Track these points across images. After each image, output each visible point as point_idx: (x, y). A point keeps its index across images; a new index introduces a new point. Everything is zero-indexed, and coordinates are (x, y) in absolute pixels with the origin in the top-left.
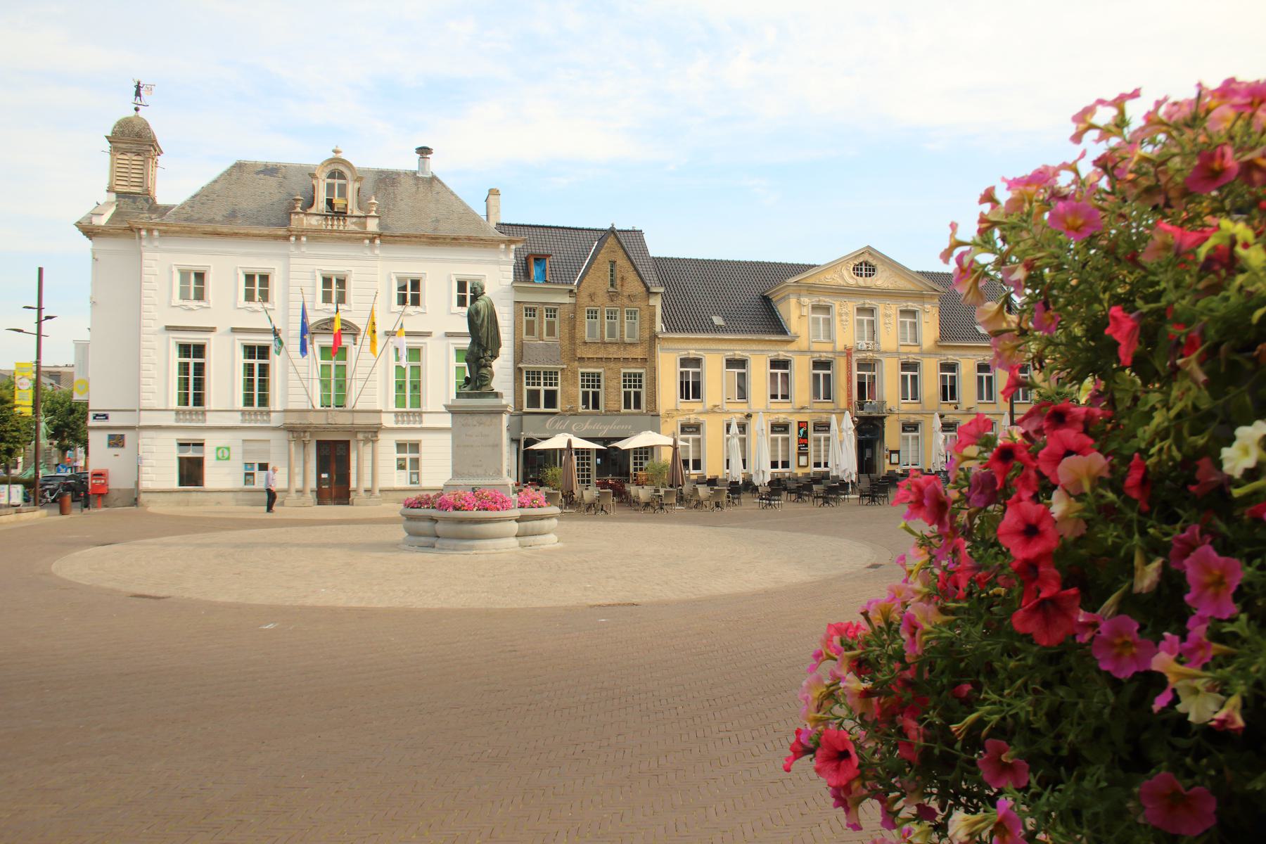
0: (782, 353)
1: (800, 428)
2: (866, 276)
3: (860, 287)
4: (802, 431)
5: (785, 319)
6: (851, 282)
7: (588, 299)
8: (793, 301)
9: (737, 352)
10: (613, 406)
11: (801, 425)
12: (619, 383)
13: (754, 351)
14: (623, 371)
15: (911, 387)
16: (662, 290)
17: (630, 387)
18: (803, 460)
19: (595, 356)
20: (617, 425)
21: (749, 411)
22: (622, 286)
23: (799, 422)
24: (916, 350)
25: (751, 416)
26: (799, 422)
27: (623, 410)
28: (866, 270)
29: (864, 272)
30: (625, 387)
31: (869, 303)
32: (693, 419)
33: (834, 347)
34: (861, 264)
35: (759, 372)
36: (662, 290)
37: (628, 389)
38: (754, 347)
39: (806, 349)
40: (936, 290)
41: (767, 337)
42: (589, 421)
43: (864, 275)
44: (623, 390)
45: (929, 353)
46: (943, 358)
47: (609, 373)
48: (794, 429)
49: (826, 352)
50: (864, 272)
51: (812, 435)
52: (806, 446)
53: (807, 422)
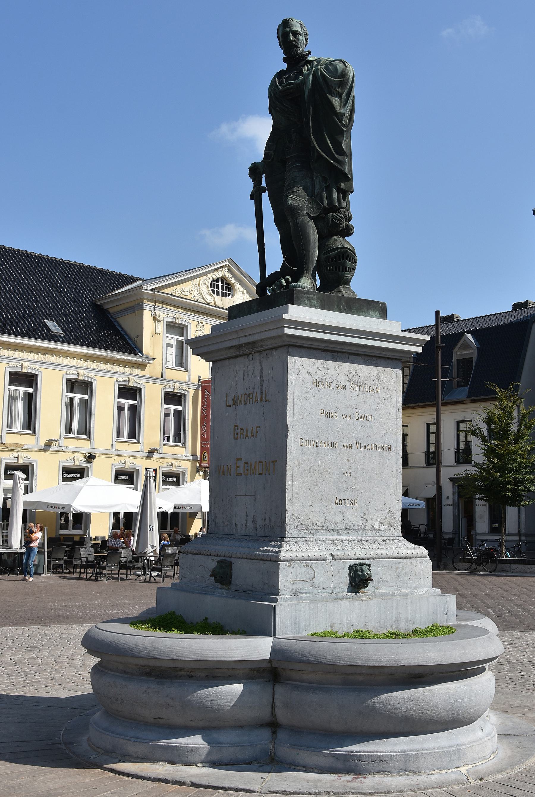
2: (222, 293)
5: (133, 336)
9: (81, 371)
13: (101, 371)
21: (91, 451)
25: (94, 458)
28: (222, 289)
32: (23, 457)
33: (188, 377)
34: (218, 280)
38: (102, 366)
41: (118, 356)
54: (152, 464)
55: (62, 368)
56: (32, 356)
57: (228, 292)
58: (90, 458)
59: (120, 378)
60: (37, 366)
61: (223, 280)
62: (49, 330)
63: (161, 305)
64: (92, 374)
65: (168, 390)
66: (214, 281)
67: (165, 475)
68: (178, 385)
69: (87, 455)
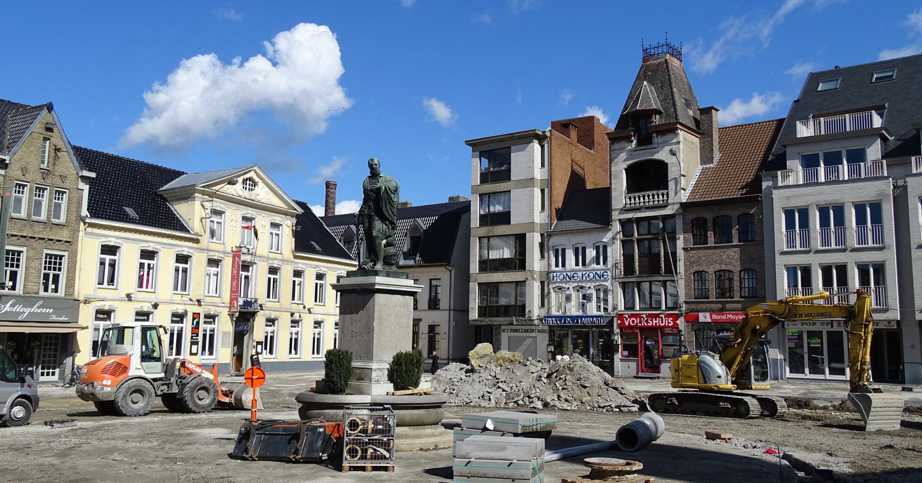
0: (185, 248)
1: (194, 319)
2: (249, 190)
3: (246, 198)
4: (195, 323)
5: (186, 218)
6: (241, 193)
7: (20, 173)
8: (197, 203)
10: (32, 287)
11: (196, 316)
12: (41, 264)
14: (46, 251)
15: (272, 288)
16: (93, 175)
17: (50, 269)
18: (194, 348)
19: (20, 234)
20: (38, 308)
21: (156, 301)
22: (54, 164)
23: (194, 313)
24: (279, 256)
25: (158, 305)
26: (194, 313)
27: (42, 293)
28: (249, 185)
29: (248, 187)
30: (45, 269)
31: (250, 212)
32: (106, 306)
34: (247, 180)
35: (166, 263)
36: (93, 175)
37: (47, 271)
38: (165, 240)
39: (205, 248)
40: (296, 210)
42: (10, 303)
43: (248, 189)
44: (43, 271)
45: (287, 261)
46: (296, 266)
47: (32, 253)
48: (190, 317)
49: (219, 252)
50: (248, 187)
51: (202, 326)
52: (197, 335)
53: (199, 314)
54: (197, 309)
55: (137, 242)
56: (117, 234)
57: (253, 188)
58: (155, 306)
59: (178, 249)
60: (120, 241)
61: (250, 179)
62: (128, 215)
63: (200, 195)
64: (158, 247)
65: (210, 257)
66: (244, 180)
67: (206, 317)
68: (217, 254)
69: (153, 303)
